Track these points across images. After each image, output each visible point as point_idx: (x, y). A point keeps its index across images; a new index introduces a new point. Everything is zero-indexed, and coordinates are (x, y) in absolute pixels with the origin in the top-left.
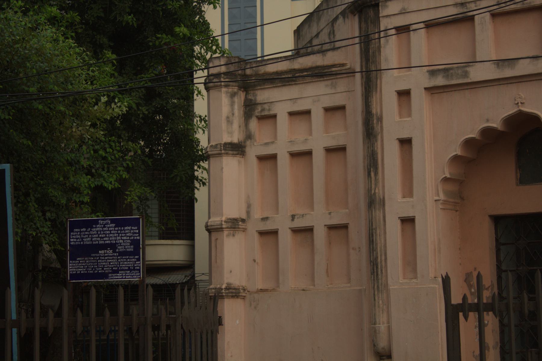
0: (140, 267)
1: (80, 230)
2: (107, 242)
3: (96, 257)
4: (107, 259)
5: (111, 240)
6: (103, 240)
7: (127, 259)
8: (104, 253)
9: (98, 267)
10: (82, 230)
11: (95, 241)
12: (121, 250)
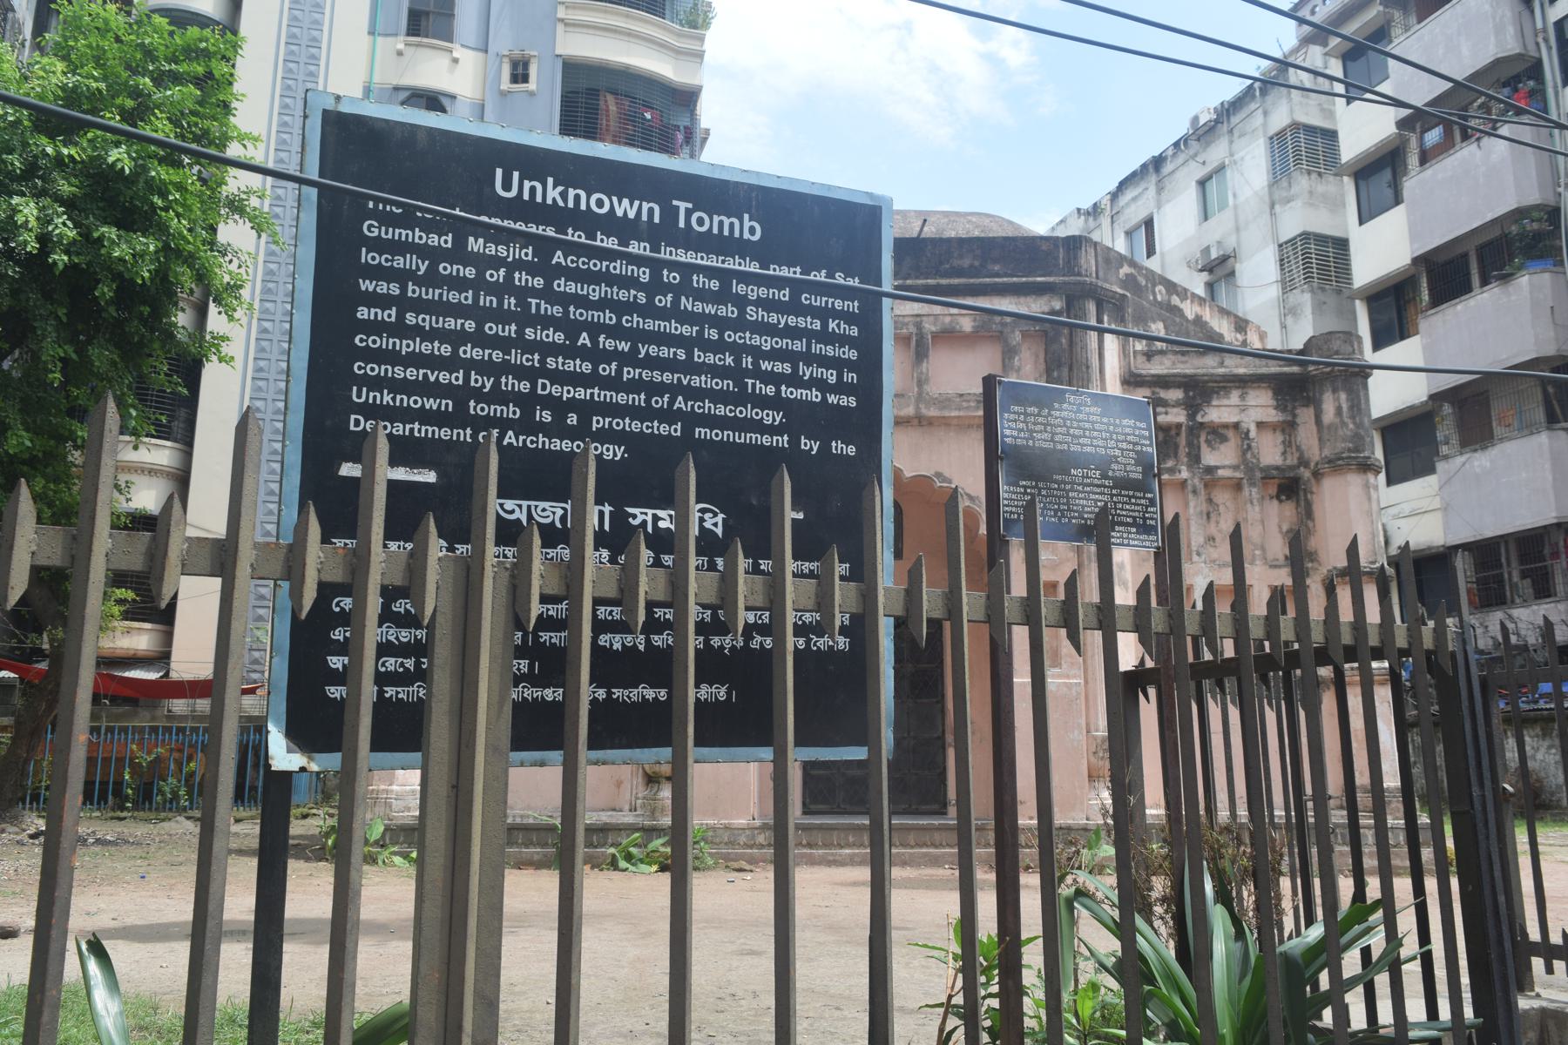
0: (1156, 520)
1: (1025, 410)
2: (1089, 449)
3: (1066, 483)
4: (1089, 493)
5: (1096, 447)
6: (1079, 444)
7: (1130, 497)
8: (1083, 477)
9: (1069, 510)
10: (1030, 410)
11: (1061, 443)
12: (1117, 474)
